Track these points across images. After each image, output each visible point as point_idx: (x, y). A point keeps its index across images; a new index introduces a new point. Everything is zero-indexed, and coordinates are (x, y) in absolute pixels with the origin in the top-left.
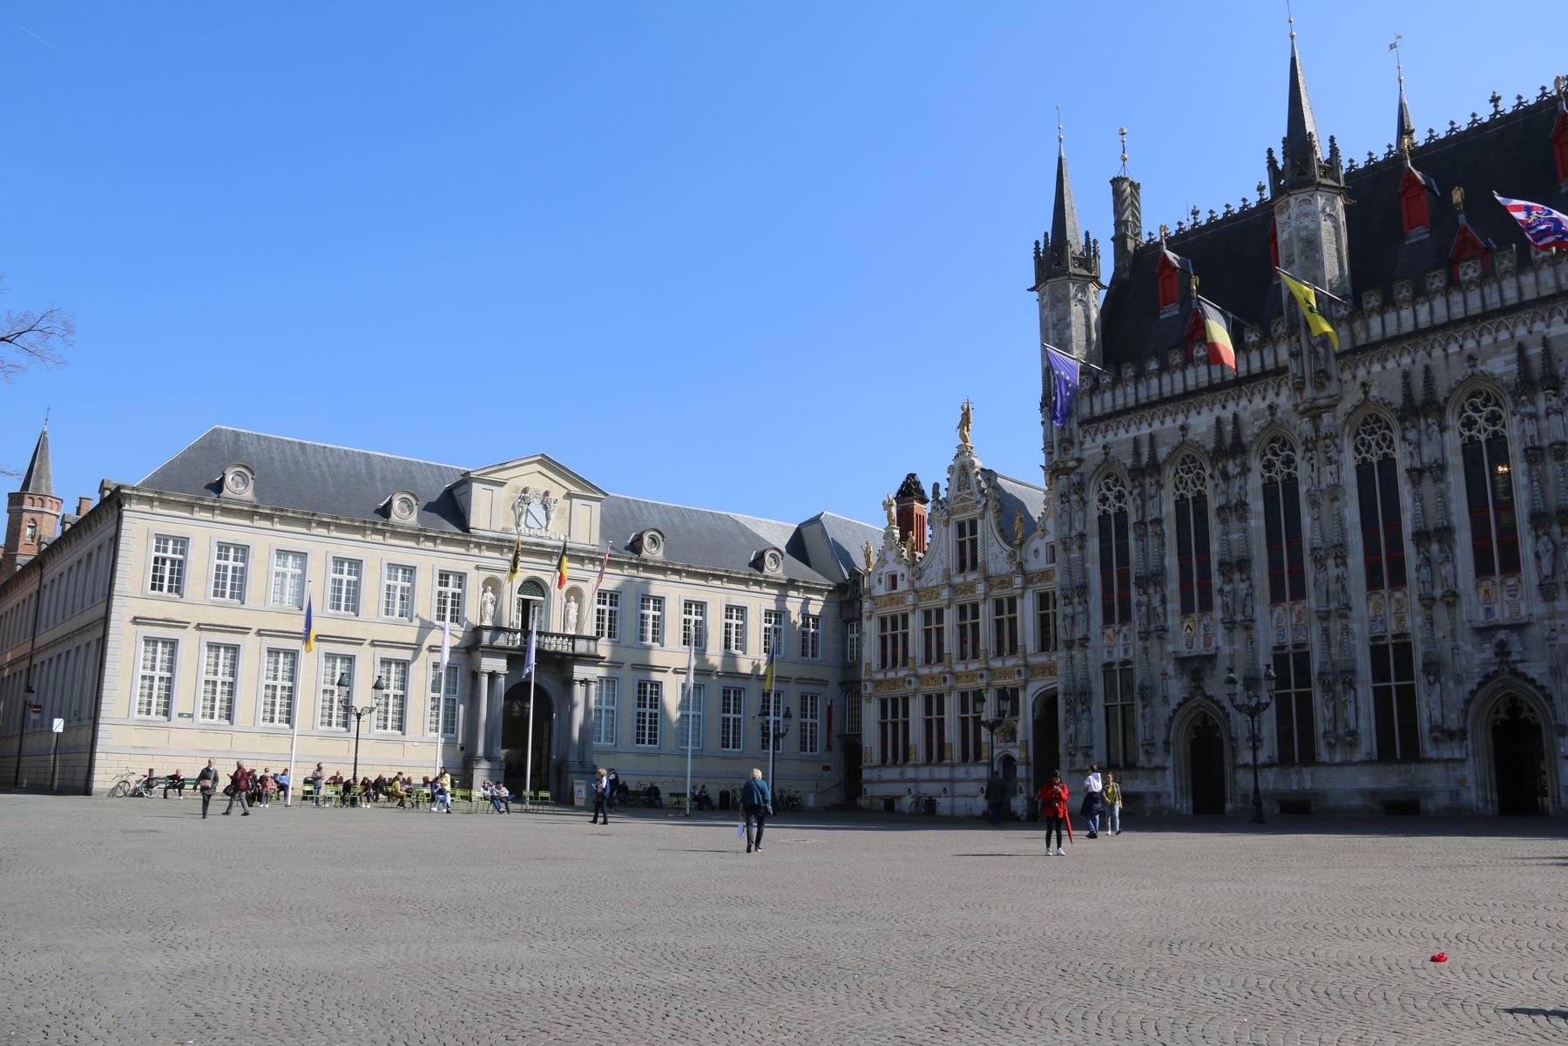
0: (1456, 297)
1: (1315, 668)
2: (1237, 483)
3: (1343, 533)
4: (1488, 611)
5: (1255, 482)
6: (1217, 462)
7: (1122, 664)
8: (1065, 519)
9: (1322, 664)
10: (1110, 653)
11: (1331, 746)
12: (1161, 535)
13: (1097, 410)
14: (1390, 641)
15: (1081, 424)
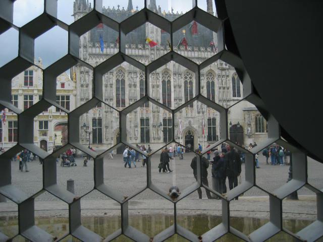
0: (186, 52)
1: (151, 122)
2: (135, 79)
3: (159, 95)
4: (187, 114)
5: (138, 80)
6: (130, 73)
7: (99, 117)
8: (83, 78)
9: (153, 121)
10: (94, 115)
11: (154, 139)
12: (111, 87)
13: (94, 52)
14: (167, 118)
15: (89, 54)
